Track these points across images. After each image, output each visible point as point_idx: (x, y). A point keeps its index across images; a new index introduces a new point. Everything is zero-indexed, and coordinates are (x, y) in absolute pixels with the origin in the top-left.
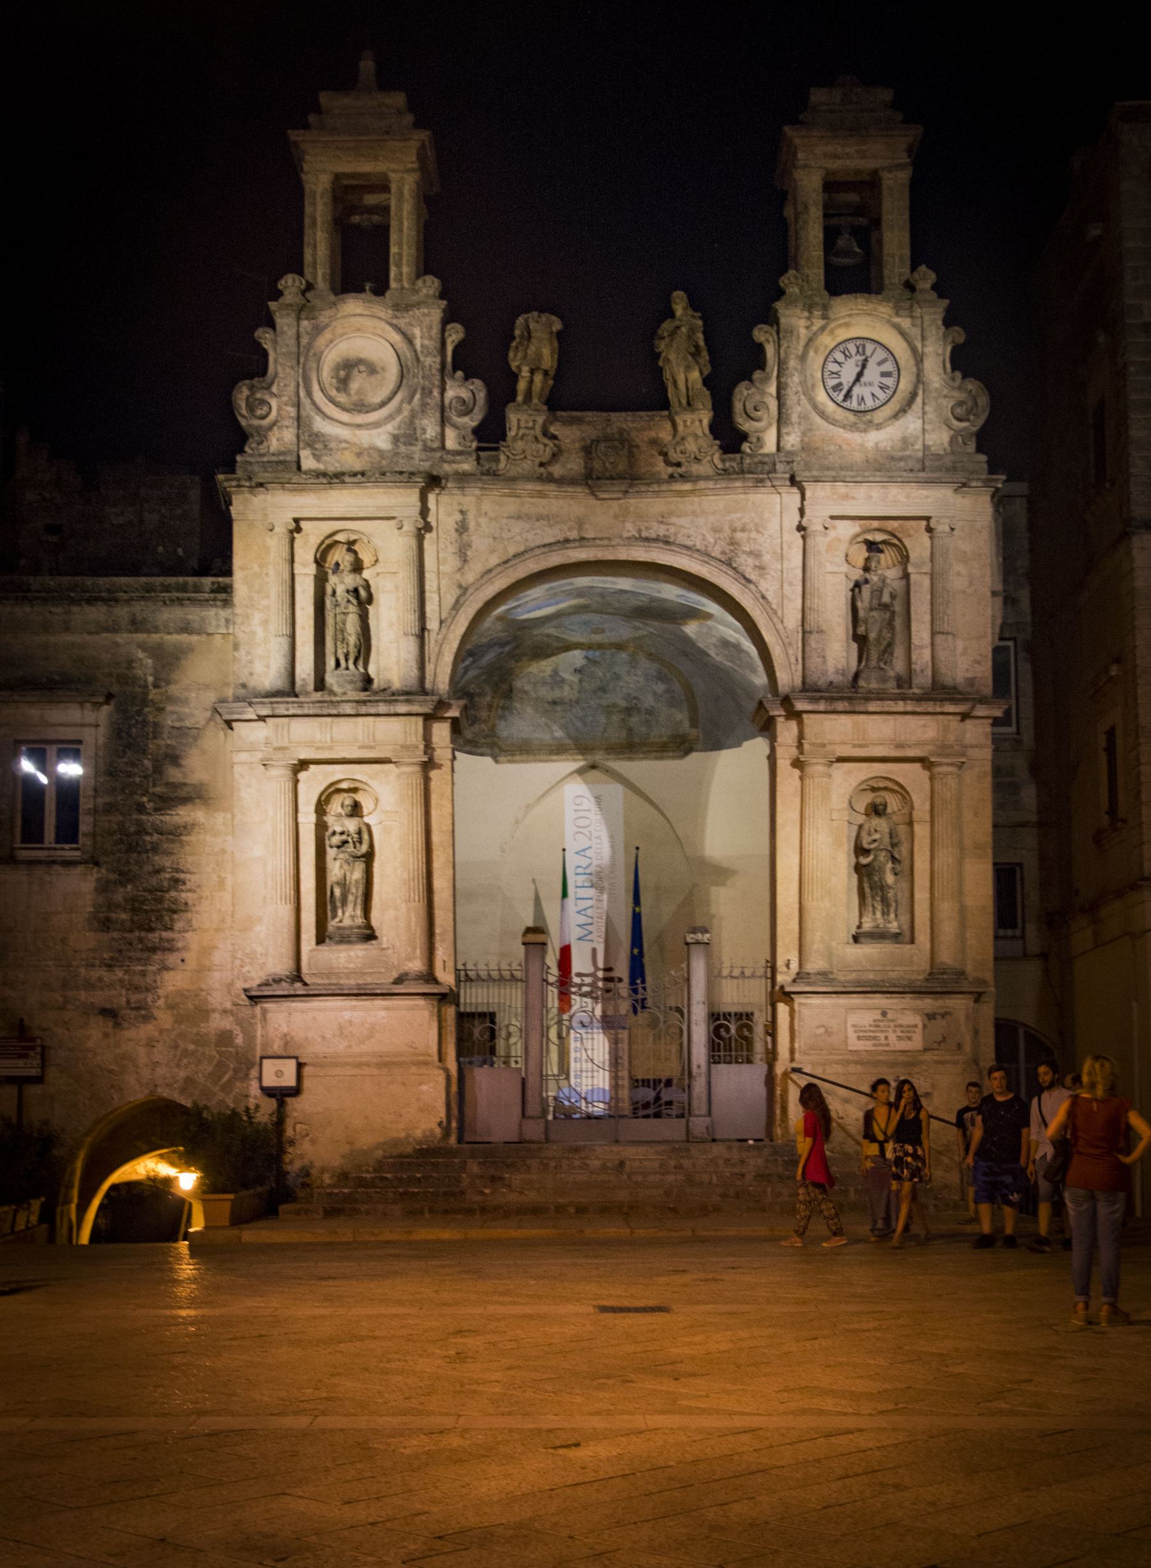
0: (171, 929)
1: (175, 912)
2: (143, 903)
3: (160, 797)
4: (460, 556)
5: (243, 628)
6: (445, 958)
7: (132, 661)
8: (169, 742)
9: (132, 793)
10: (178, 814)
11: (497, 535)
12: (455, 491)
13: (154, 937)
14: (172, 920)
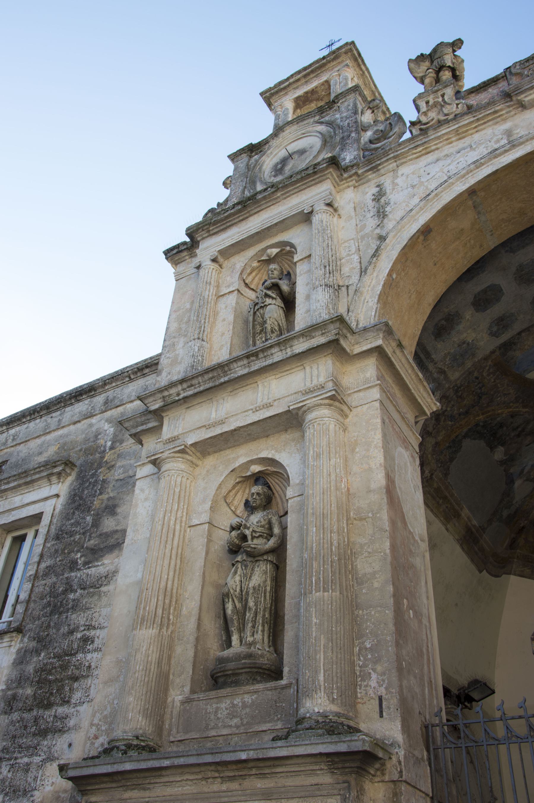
0: (66, 702)
1: (76, 679)
2: (50, 673)
3: (92, 549)
4: (379, 216)
5: (168, 355)
6: (382, 691)
7: (99, 434)
8: (111, 495)
9: (69, 553)
10: (103, 564)
11: (415, 183)
12: (371, 175)
13: (48, 714)
14: (71, 690)
